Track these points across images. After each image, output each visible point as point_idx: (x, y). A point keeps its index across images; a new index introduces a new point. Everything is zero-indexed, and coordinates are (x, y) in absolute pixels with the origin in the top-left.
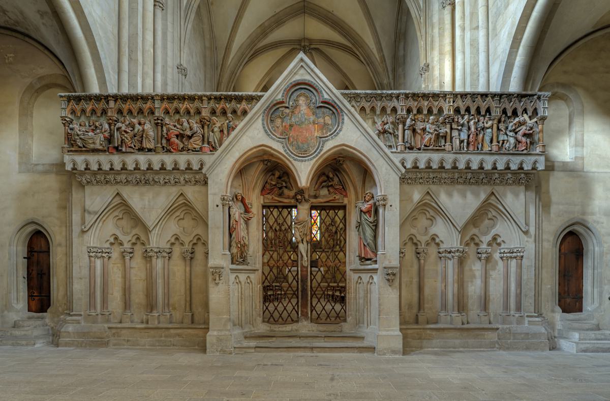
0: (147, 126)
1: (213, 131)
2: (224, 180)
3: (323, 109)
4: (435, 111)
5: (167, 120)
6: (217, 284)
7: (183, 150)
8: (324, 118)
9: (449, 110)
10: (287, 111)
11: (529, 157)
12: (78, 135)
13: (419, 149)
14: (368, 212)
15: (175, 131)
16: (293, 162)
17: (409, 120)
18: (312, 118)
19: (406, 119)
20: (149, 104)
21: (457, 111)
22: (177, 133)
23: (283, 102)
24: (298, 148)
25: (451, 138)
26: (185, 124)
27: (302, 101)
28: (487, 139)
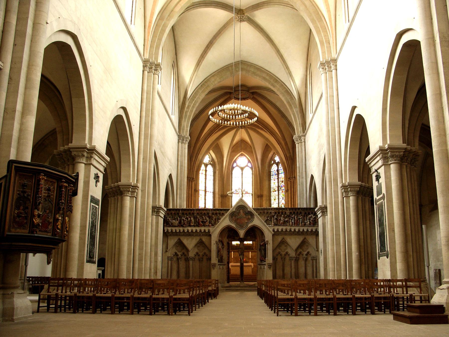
0: (192, 219)
1: (213, 220)
2: (217, 236)
3: (248, 214)
4: (284, 213)
5: (198, 217)
6: (214, 269)
7: (203, 226)
8: (248, 216)
9: (288, 213)
10: (237, 214)
11: (314, 227)
12: (170, 221)
13: (279, 225)
14: (263, 245)
15: (201, 220)
16: (239, 230)
17: (275, 216)
18: (245, 216)
19: (274, 216)
20: (193, 212)
21: (291, 213)
22: (201, 221)
23: (235, 212)
24: (240, 225)
25: (289, 221)
26: (204, 218)
27: (241, 211)
28: (301, 222)
